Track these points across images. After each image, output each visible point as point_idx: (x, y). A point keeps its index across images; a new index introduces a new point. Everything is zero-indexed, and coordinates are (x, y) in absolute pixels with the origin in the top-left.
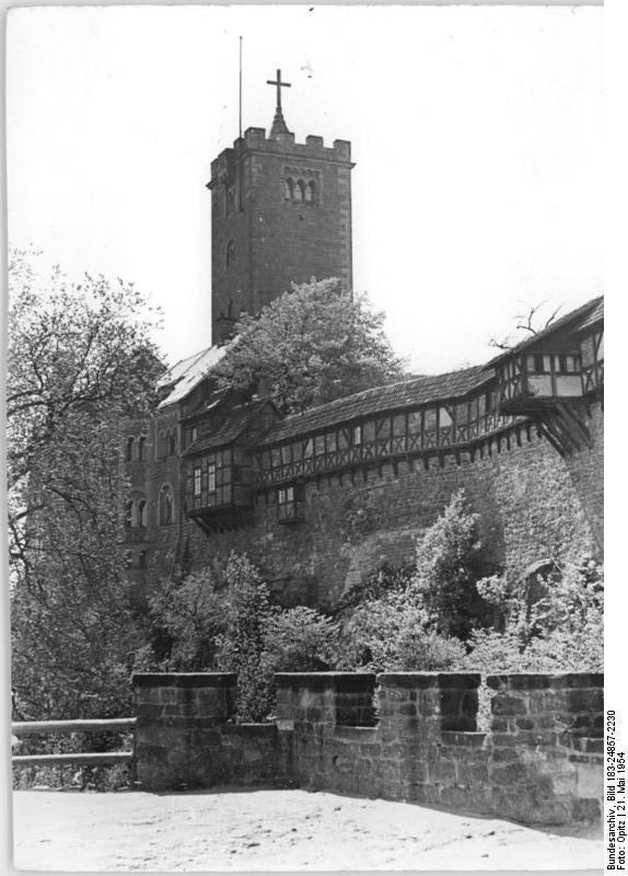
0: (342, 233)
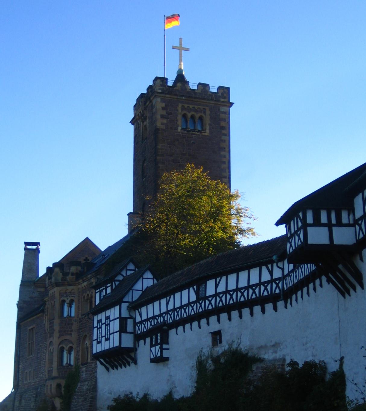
0: (222, 153)
